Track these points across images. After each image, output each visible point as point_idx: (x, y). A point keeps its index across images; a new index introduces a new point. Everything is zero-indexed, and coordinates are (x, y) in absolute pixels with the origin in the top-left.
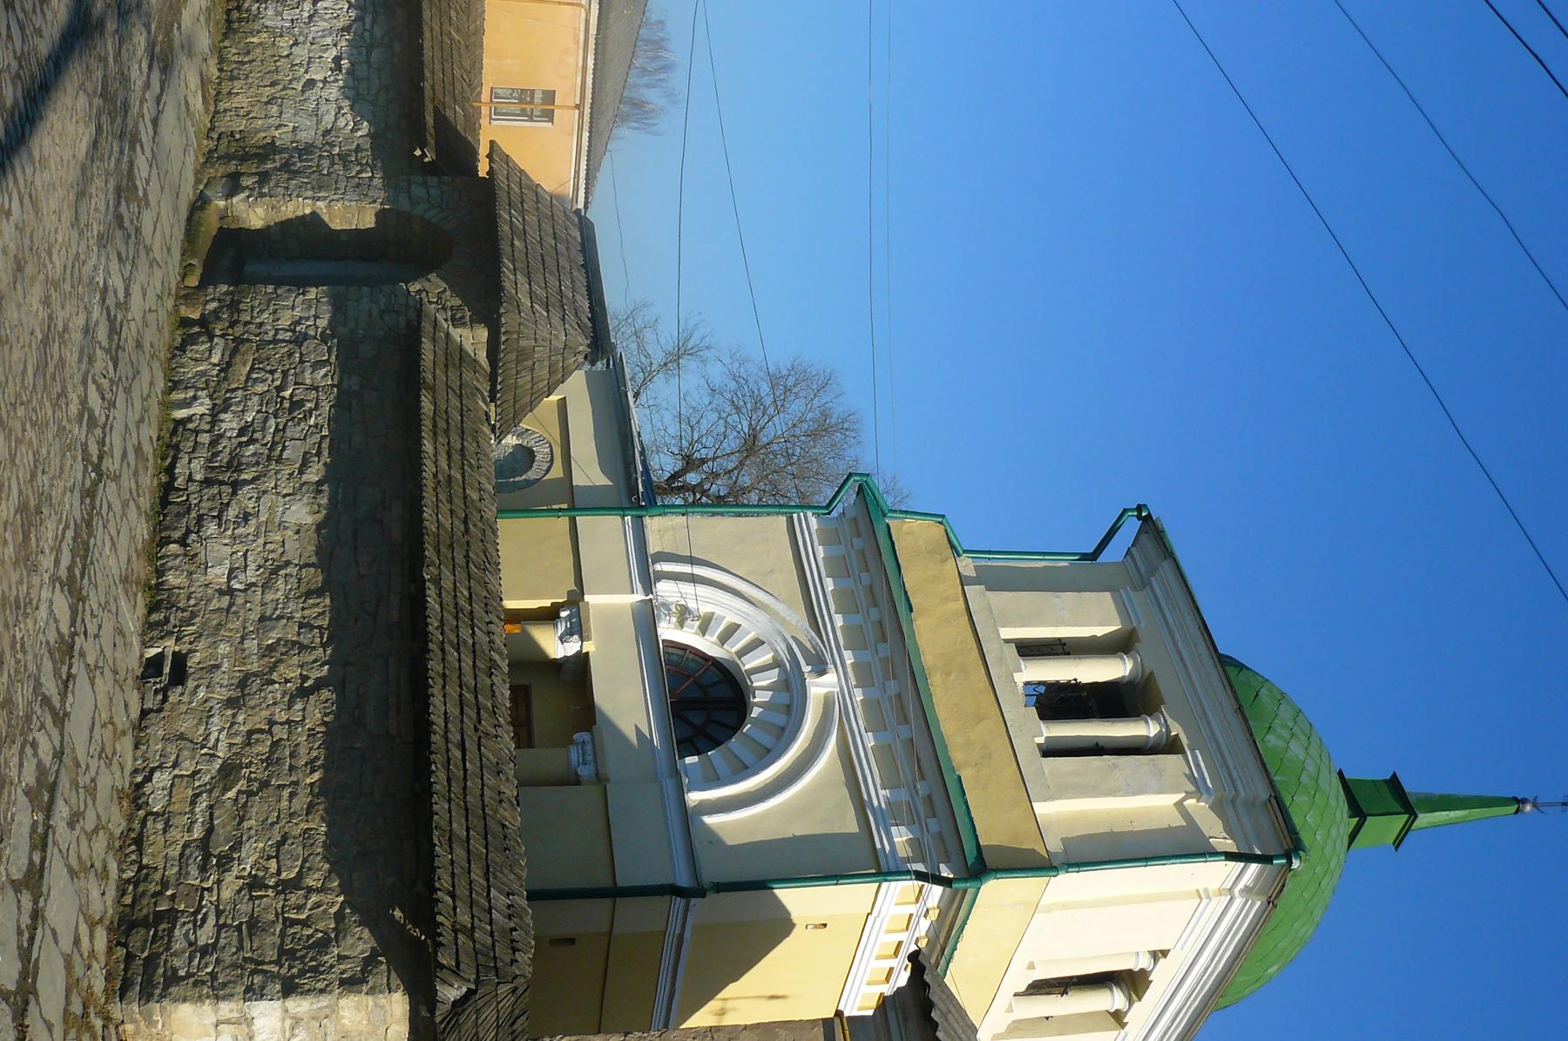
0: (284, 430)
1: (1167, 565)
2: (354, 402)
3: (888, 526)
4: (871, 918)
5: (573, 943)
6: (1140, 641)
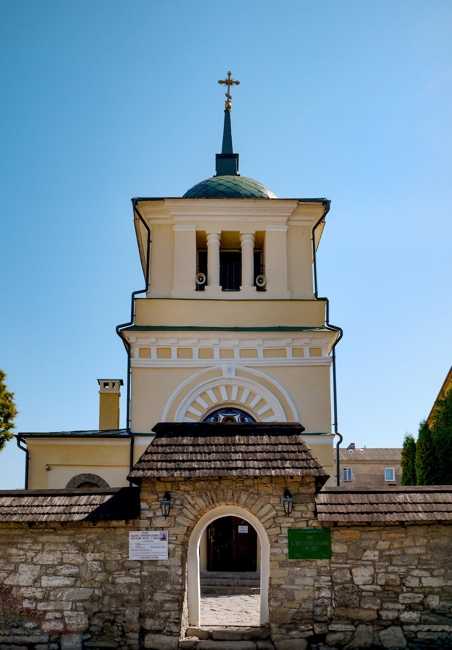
0: (413, 589)
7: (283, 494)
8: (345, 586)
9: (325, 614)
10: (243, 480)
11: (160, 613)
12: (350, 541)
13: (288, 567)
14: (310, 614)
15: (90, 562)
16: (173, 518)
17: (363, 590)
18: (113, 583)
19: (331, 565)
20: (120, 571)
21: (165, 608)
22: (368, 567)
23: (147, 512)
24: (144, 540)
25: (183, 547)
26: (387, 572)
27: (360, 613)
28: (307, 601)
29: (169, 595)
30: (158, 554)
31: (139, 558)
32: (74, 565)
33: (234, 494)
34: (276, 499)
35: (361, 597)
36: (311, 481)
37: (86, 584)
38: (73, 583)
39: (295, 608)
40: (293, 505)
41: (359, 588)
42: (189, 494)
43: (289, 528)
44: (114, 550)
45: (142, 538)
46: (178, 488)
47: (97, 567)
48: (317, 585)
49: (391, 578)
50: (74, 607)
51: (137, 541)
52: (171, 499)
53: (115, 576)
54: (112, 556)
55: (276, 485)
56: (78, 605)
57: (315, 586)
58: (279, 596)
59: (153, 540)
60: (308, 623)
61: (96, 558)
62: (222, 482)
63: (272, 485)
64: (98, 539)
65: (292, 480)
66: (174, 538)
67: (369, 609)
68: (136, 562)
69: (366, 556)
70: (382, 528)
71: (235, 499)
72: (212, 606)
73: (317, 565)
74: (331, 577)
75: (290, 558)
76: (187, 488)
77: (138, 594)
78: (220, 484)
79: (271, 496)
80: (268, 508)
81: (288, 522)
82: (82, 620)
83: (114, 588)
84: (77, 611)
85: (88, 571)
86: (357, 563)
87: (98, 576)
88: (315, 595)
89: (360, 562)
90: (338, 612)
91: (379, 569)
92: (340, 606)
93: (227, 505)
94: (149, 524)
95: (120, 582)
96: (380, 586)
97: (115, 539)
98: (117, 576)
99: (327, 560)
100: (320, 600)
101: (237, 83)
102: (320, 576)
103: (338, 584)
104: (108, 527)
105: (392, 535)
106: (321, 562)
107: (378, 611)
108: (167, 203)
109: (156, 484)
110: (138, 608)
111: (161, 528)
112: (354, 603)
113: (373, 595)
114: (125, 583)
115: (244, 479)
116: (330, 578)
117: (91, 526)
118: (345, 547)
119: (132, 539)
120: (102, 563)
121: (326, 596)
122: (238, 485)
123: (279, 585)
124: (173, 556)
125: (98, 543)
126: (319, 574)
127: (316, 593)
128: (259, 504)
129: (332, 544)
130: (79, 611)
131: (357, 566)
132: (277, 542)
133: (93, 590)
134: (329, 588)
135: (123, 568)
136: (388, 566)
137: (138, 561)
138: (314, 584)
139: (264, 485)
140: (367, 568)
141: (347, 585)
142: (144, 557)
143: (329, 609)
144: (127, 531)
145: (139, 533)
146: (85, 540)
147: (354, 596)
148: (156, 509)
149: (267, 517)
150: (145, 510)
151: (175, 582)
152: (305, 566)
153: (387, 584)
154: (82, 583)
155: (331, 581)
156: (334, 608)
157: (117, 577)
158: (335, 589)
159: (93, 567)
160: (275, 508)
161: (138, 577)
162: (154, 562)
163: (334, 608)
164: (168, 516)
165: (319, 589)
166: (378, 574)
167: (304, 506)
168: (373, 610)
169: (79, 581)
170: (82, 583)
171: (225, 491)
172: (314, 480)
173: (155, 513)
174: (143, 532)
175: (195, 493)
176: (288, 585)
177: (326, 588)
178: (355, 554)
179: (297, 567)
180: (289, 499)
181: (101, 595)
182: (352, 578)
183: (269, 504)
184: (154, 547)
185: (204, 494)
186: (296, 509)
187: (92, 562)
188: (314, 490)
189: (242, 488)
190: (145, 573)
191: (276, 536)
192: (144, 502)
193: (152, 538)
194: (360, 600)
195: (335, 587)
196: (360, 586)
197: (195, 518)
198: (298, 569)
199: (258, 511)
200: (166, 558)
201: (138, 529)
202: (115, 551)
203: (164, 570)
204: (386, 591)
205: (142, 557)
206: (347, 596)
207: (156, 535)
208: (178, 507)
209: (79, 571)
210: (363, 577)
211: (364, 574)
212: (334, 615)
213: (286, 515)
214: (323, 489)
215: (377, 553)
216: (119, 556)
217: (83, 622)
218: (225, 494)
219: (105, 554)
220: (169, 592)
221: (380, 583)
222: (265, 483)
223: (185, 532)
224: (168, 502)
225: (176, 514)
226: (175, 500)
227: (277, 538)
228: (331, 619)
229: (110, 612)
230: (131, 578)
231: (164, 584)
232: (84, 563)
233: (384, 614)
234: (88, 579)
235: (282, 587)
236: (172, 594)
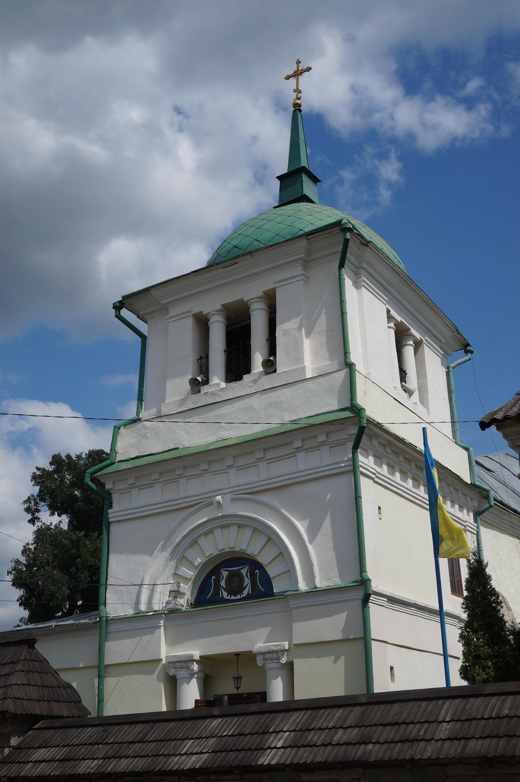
1: (154, 293)
3: (119, 462)
4: (376, 479)
5: (393, 667)
6: (202, 312)
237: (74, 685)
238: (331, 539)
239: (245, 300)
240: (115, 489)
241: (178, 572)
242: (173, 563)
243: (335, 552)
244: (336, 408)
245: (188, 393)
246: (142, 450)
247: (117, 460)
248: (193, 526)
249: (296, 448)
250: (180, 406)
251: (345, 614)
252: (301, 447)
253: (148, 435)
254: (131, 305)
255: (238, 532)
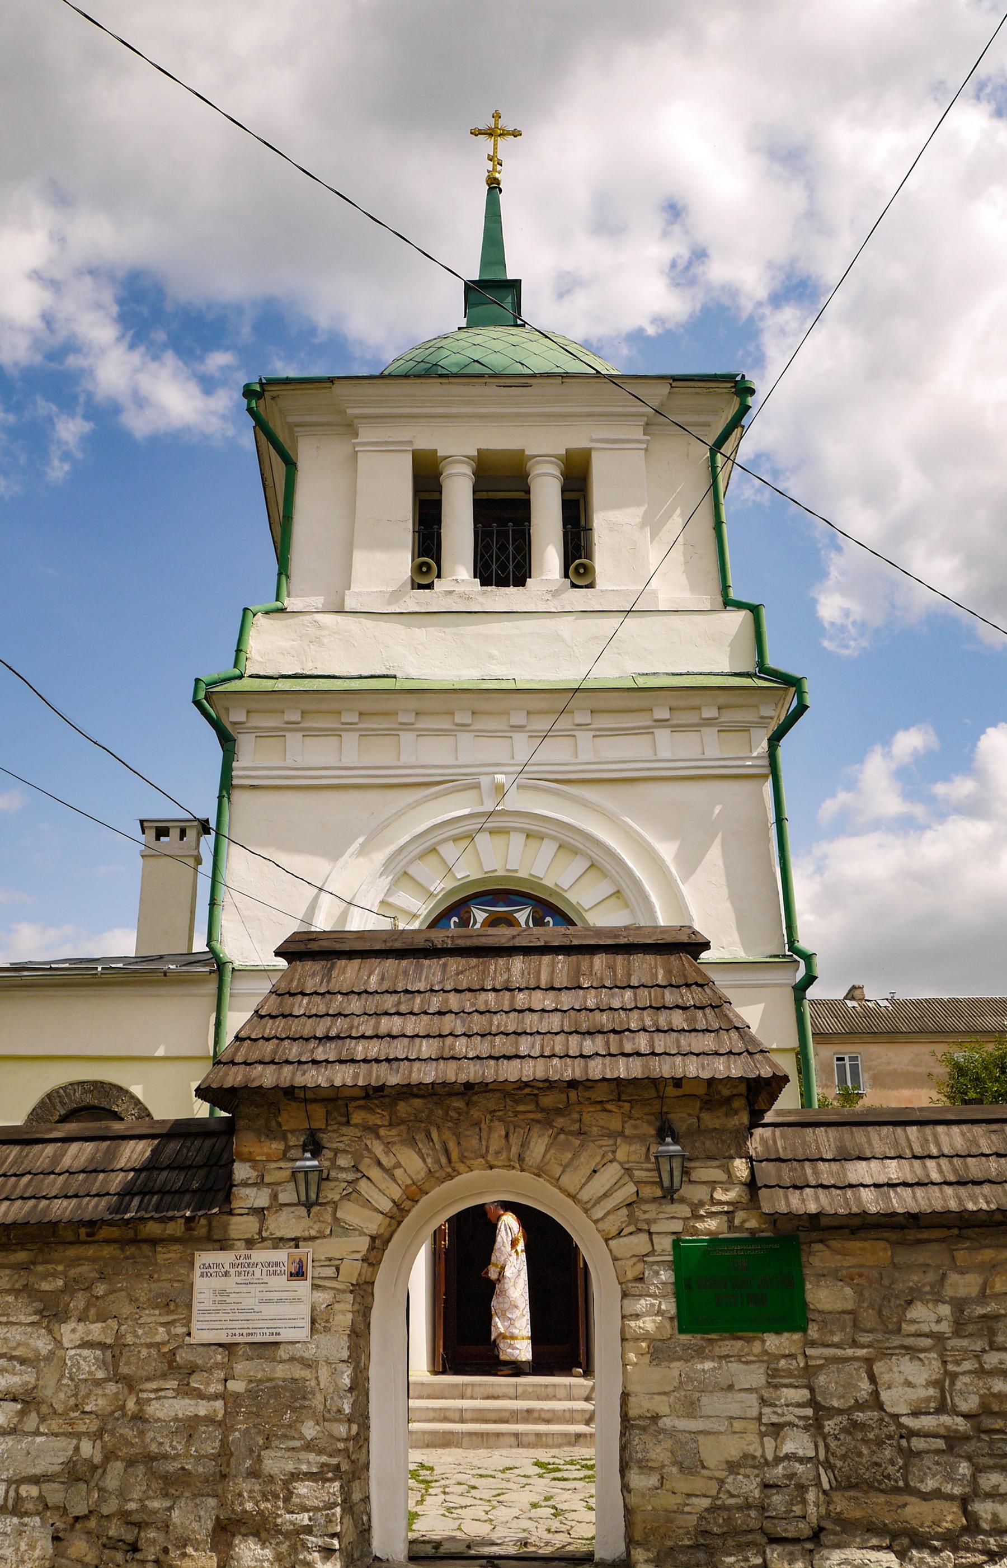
2: (980, 1311)
7: (653, 1132)
8: (855, 1417)
9: (799, 1513)
10: (536, 1092)
11: (281, 1516)
12: (861, 1275)
13: (679, 1359)
14: (753, 1514)
15: (72, 1352)
16: (330, 1210)
17: (912, 1433)
18: (139, 1418)
19: (809, 1352)
20: (164, 1376)
21: (295, 1500)
22: (922, 1356)
23: (251, 1192)
24: (239, 1280)
25: (359, 1299)
26: (981, 1372)
27: (908, 1509)
28: (742, 1471)
29: (312, 1457)
30: (279, 1323)
31: (224, 1339)
32: (23, 1361)
33: (511, 1135)
34: (633, 1148)
35: (910, 1455)
36: (735, 1092)
37: (55, 1425)
38: (15, 1420)
39: (705, 1496)
40: (686, 1164)
41: (900, 1425)
42: (378, 1137)
43: (674, 1237)
44: (147, 1312)
45: (232, 1271)
46: (344, 1119)
47: (93, 1368)
48: (770, 1416)
49: (996, 1389)
50: (10, 1502)
51: (217, 1283)
52: (325, 1151)
53: (144, 1395)
54: (140, 1332)
55: (632, 1107)
56: (24, 1495)
57: (764, 1421)
58: (654, 1457)
59: (266, 1279)
60: (749, 1545)
61: (90, 1338)
62: (475, 1098)
63: (620, 1107)
64: (102, 1277)
65: (679, 1092)
66: (330, 1272)
67: (937, 1494)
68: (213, 1348)
69: (913, 1322)
70: (956, 1231)
71: (514, 1150)
72: (447, 1490)
73: (765, 1352)
74: (812, 1390)
75: (682, 1331)
76: (374, 1119)
77: (212, 1454)
78: (467, 1104)
79: (619, 1140)
80: (611, 1173)
81: (672, 1218)
82: (32, 1547)
83: (142, 1433)
84: (22, 1514)
85: (65, 1381)
86: (887, 1345)
87: (92, 1398)
88: (764, 1451)
89: (896, 1341)
90: (841, 1504)
91: (957, 1363)
92: (846, 1485)
93: (491, 1168)
94: (257, 1231)
95: (160, 1415)
96: (966, 1416)
97: (151, 1277)
98: (152, 1396)
99: (797, 1336)
100: (780, 1467)
101: (516, 134)
102: (776, 1387)
103: (832, 1412)
104: (135, 1241)
105: (987, 1255)
106: (777, 1342)
107: (964, 1501)
108: (338, 389)
109: (281, 1107)
110: (212, 1502)
111: (293, 1239)
112: (888, 1477)
113: (944, 1447)
114: (176, 1419)
115: (539, 1088)
116: (806, 1392)
117: (83, 1237)
118: (848, 1291)
119: (202, 1276)
120: (109, 1353)
121: (801, 1453)
122: (521, 1108)
123: (656, 1418)
124: (327, 1330)
125: (100, 1289)
126: (774, 1378)
127: (769, 1442)
128: (587, 1161)
129: (807, 1283)
130: (26, 1514)
131: (885, 1354)
132: (640, 1279)
133: (75, 1442)
134: (806, 1428)
135: (170, 1367)
136: (984, 1351)
137: (219, 1345)
138: (761, 1414)
139: (599, 1107)
140: (921, 1360)
141: (860, 1416)
142: (237, 1332)
143: (811, 1496)
144: (189, 1252)
145: (225, 1258)
146: (60, 1283)
147: (888, 1453)
148: (279, 1184)
149: (610, 1203)
150: (245, 1184)
151: (329, 1411)
152: (728, 1356)
153: (986, 1409)
154: (43, 1419)
155: (813, 1402)
156: (825, 1492)
157: (150, 1400)
158: (827, 1429)
159: (78, 1369)
160: (631, 1176)
161: (216, 1397)
162: (267, 1349)
163: (825, 1492)
164: (317, 1203)
165: (776, 1429)
166: (954, 1376)
167: (718, 1167)
168: (950, 1498)
169: (34, 1415)
170: (43, 1419)
171: (483, 1126)
172: (742, 1089)
173: (275, 1197)
174: (238, 1253)
175: (394, 1132)
176: (678, 1417)
177: (797, 1426)
178: (880, 1313)
179: (706, 1358)
180: (672, 1148)
181: (97, 1459)
182: (876, 1394)
183: (615, 1164)
184: (269, 1301)
185: (420, 1136)
186: (694, 1177)
187: (78, 1351)
188: (745, 1118)
189: (531, 1116)
190: (236, 1386)
191: (639, 1261)
192: (244, 1160)
193: (264, 1273)
194: (905, 1467)
195: (826, 1423)
196: (903, 1420)
197: (395, 1209)
198: (708, 1365)
199: (584, 1185)
200: (304, 1334)
201: (223, 1244)
202: (151, 1316)
203: (298, 1372)
204: (985, 1432)
205: (230, 1332)
206: (865, 1451)
207: (277, 1264)
208: (343, 1176)
209: (38, 1379)
210: (909, 1390)
211: (910, 1378)
212: (828, 1515)
213: (664, 1197)
214: (769, 1117)
215: (945, 1310)
216: (161, 1330)
217: (37, 1553)
218: (484, 1134)
219: (120, 1324)
220: (309, 1446)
221: (964, 1407)
222: (601, 1102)
223: (364, 1253)
224: (315, 1163)
225: (337, 1197)
226: (336, 1154)
227: (640, 1266)
228: (820, 1530)
229: (124, 1516)
230: (192, 1402)
231: (295, 1421)
232: (52, 1353)
233: (984, 1509)
234: (59, 1408)
235: (661, 1423)
236: (320, 1452)
237: (137, 1090)
238: (723, 881)
239: (527, 453)
240: (248, 725)
241: (390, 900)
242: (386, 882)
243: (732, 903)
244: (727, 669)
245: (404, 585)
246: (310, 665)
247: (248, 673)
248: (439, 820)
249: (656, 721)
250: (389, 603)
251: (763, 1005)
252: (667, 720)
253: (325, 641)
254: (273, 398)
255: (526, 845)
